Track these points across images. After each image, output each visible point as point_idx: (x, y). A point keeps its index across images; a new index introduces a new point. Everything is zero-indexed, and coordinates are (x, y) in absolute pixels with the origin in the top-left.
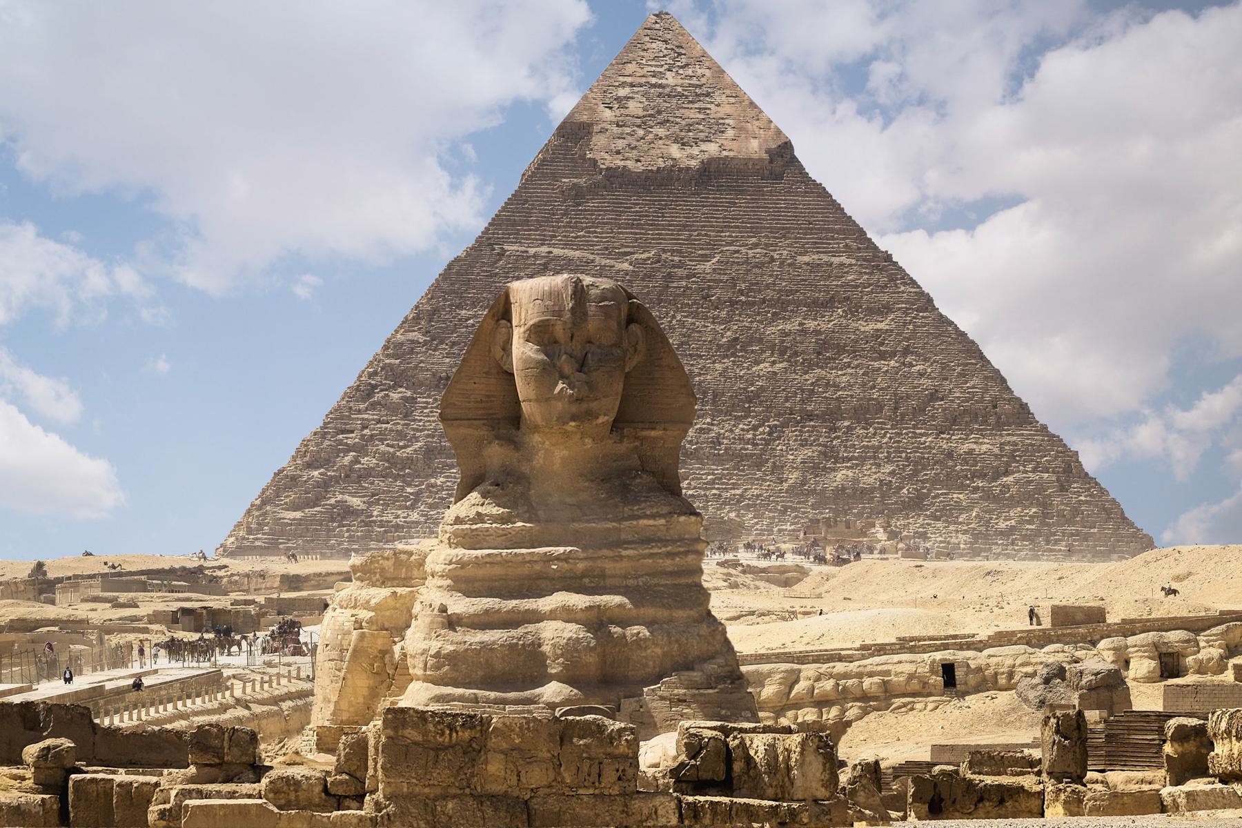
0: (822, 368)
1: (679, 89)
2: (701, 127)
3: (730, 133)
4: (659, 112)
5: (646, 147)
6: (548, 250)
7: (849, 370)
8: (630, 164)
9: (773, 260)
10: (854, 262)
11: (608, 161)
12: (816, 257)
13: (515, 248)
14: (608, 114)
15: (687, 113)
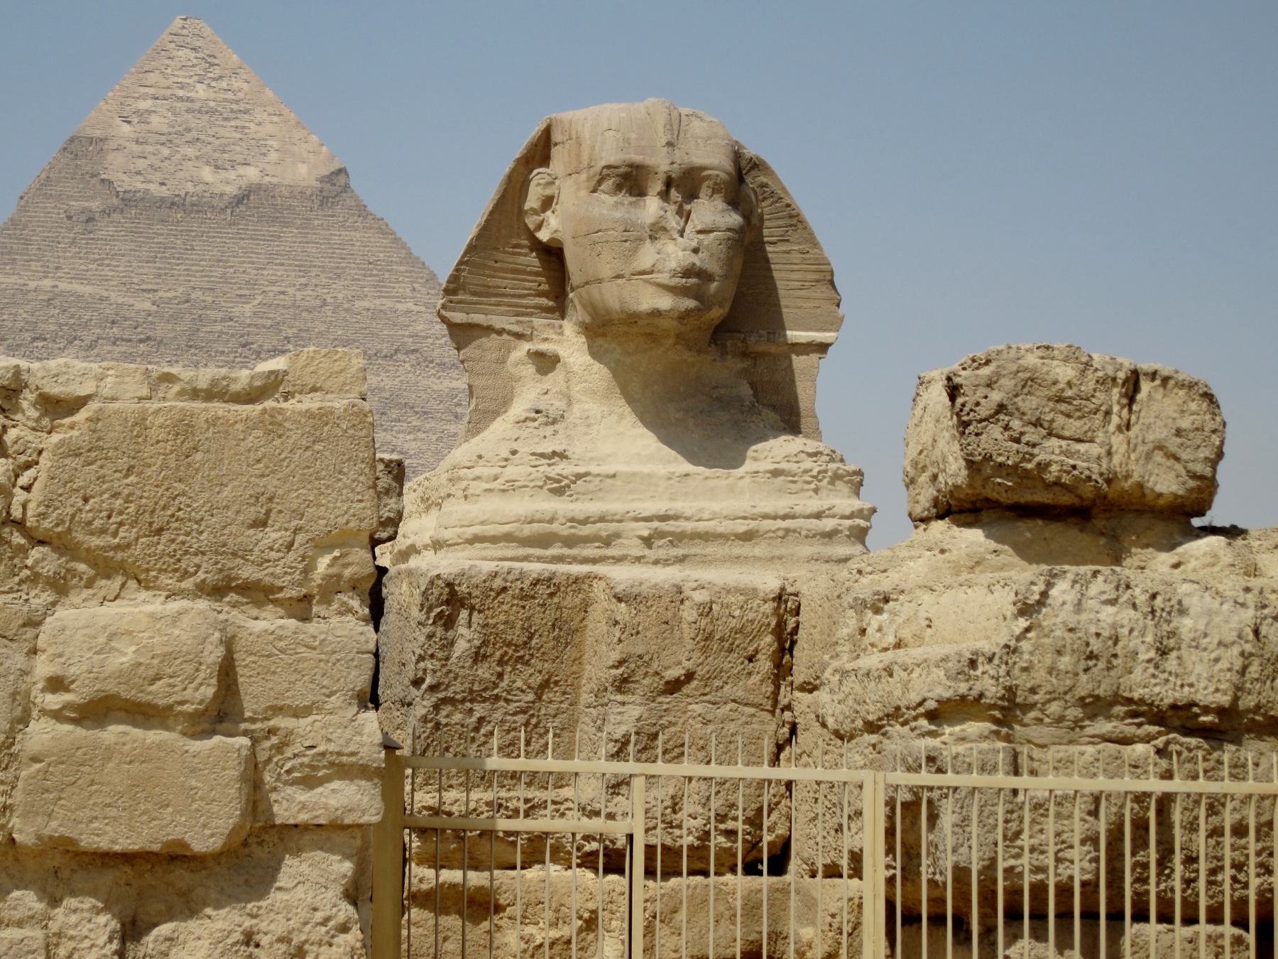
0: (386, 430)
1: (212, 104)
2: (238, 148)
3: (273, 156)
4: (189, 130)
5: (172, 169)
6: (53, 283)
7: (423, 436)
8: (151, 187)
9: (324, 303)
10: (423, 309)
11: (125, 183)
12: (378, 302)
13: (13, 279)
14: (126, 128)
15: (221, 132)
